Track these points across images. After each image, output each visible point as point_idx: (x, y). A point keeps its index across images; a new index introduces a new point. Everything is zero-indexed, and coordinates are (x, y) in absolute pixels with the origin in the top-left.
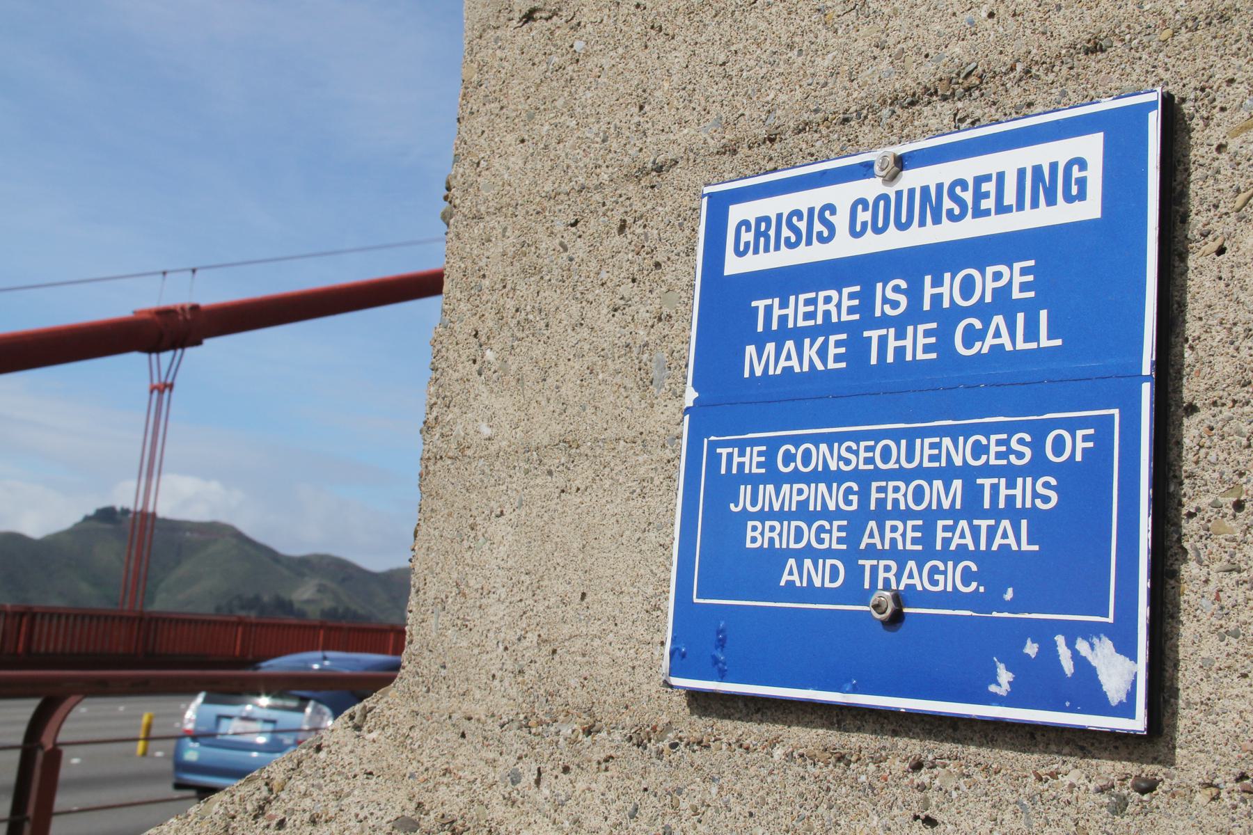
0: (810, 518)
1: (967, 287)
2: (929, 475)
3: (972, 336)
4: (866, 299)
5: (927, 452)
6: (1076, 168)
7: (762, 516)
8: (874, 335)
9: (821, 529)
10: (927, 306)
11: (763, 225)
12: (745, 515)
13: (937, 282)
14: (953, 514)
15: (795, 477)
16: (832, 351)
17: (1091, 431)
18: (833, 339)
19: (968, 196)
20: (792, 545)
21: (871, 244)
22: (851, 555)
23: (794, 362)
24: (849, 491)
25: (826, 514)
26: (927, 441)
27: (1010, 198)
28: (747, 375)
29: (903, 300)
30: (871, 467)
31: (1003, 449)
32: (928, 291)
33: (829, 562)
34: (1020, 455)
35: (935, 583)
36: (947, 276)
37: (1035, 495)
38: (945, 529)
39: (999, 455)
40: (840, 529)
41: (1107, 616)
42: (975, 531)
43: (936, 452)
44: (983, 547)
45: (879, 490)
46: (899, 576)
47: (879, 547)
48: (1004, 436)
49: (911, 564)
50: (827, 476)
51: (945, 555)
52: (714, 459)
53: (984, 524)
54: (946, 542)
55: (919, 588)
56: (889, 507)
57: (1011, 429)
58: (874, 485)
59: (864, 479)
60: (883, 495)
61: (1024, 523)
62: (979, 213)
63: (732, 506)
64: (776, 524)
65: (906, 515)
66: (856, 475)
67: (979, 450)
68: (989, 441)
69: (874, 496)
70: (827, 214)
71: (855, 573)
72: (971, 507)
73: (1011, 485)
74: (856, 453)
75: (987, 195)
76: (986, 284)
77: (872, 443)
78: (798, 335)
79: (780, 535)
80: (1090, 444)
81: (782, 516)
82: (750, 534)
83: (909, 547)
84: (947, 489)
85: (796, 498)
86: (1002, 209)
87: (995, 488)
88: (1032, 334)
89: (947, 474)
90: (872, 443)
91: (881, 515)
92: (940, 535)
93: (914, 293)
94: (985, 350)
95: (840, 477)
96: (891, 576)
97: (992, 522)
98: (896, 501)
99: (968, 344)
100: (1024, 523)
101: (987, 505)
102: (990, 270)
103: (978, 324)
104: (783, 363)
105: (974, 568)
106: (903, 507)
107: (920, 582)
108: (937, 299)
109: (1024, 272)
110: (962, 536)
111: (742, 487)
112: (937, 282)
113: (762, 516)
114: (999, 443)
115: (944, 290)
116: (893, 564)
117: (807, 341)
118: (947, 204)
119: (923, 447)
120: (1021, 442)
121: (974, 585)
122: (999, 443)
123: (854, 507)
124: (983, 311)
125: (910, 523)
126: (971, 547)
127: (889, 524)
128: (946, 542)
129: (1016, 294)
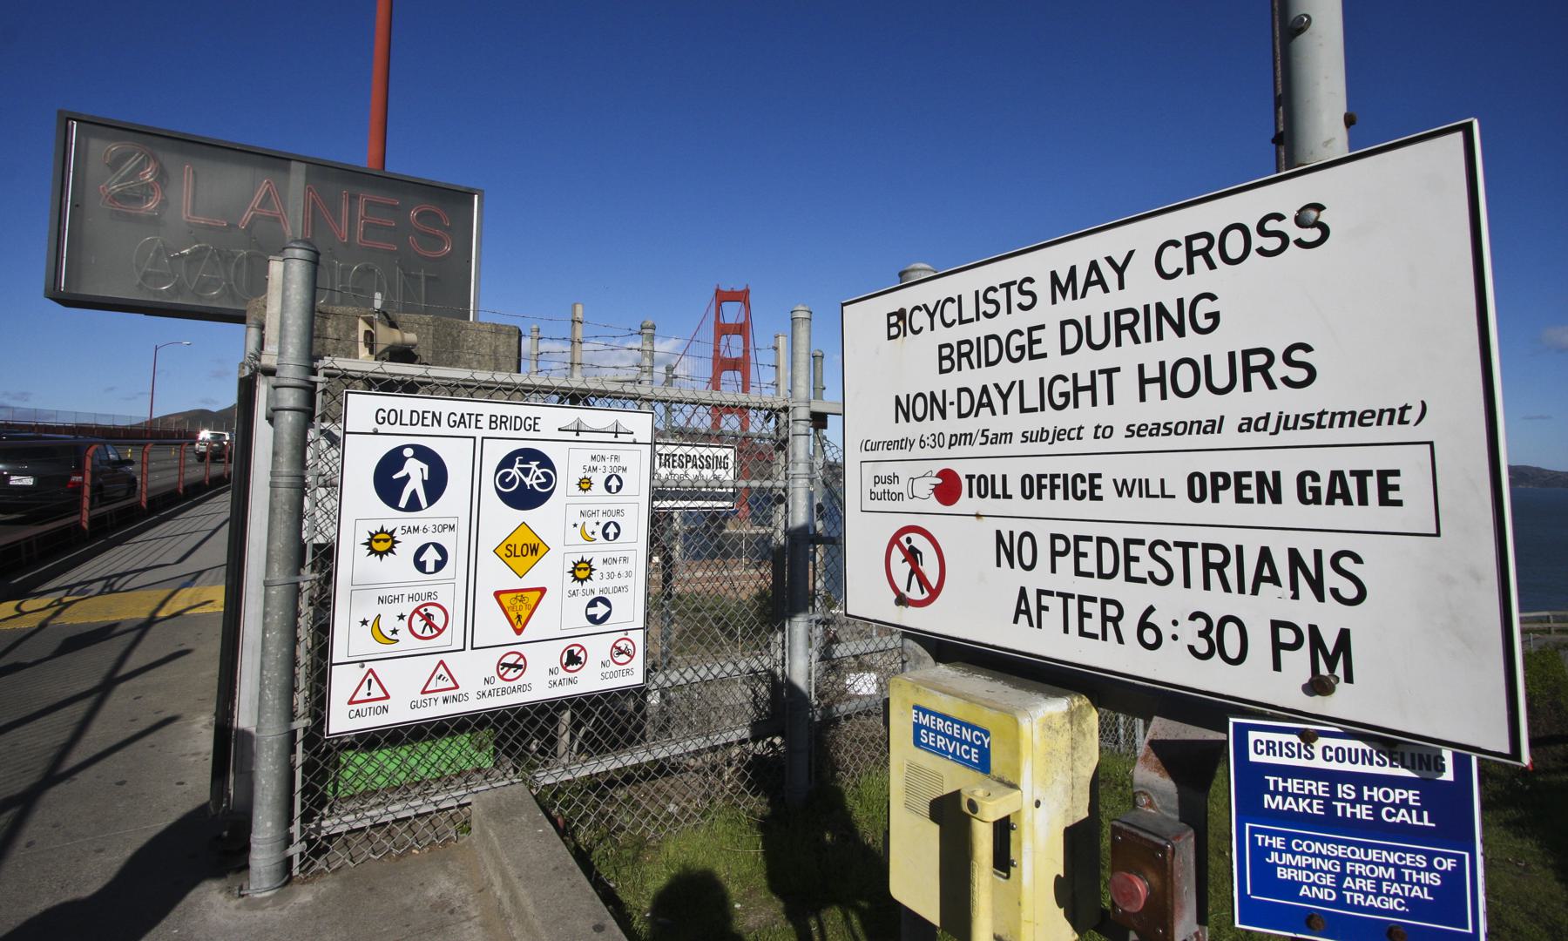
0: (1314, 872)
1: (1386, 795)
2: (1378, 864)
3: (1389, 814)
5: (1375, 856)
7: (1285, 866)
8: (1339, 805)
10: (1366, 798)
11: (1271, 745)
12: (1275, 865)
13: (1370, 790)
14: (1390, 880)
15: (1303, 853)
16: (1315, 807)
17: (1455, 861)
18: (1315, 802)
20: (1305, 880)
21: (1334, 766)
22: (1339, 889)
23: (1294, 806)
24: (1334, 864)
25: (1321, 870)
26: (1375, 851)
28: (1266, 806)
29: (1353, 795)
32: (1366, 793)
33: (1326, 890)
34: (1421, 864)
35: (1384, 905)
36: (1375, 789)
38: (1387, 885)
39: (1411, 862)
41: (1235, 724)
42: (1403, 889)
44: (1407, 894)
45: (1351, 866)
46: (1365, 900)
47: (1353, 888)
49: (1371, 897)
50: (1320, 855)
51: (1388, 894)
52: (1253, 841)
53: (1407, 887)
54: (1388, 891)
56: (1357, 873)
57: (1417, 852)
58: (1348, 864)
59: (1343, 862)
60: (1353, 868)
61: (1425, 889)
63: (1267, 860)
65: (1367, 878)
66: (1337, 858)
67: (1401, 858)
71: (1341, 898)
72: (1400, 878)
73: (1418, 873)
74: (1337, 849)
76: (1396, 795)
78: (1296, 797)
79: (1298, 875)
80: (1455, 865)
81: (1297, 867)
82: (1279, 873)
83: (1369, 890)
85: (1304, 862)
88: (1420, 818)
89: (1387, 865)
92: (1385, 889)
93: (1359, 793)
94: (1398, 821)
95: (1329, 858)
96: (1361, 900)
97: (1410, 886)
98: (1360, 872)
101: (1407, 879)
102: (1397, 791)
103: (1393, 811)
105: (1403, 902)
106: (1364, 874)
107: (1377, 904)
108: (1371, 797)
111: (1272, 853)
112: (1370, 790)
113: (1285, 866)
116: (1362, 896)
117: (1300, 800)
119: (1373, 854)
121: (1403, 908)
122: (1411, 857)
123: (1338, 870)
124: (1397, 807)
125: (1369, 881)
126: (1401, 894)
127: (1357, 880)
128: (1388, 891)
129: (1411, 803)
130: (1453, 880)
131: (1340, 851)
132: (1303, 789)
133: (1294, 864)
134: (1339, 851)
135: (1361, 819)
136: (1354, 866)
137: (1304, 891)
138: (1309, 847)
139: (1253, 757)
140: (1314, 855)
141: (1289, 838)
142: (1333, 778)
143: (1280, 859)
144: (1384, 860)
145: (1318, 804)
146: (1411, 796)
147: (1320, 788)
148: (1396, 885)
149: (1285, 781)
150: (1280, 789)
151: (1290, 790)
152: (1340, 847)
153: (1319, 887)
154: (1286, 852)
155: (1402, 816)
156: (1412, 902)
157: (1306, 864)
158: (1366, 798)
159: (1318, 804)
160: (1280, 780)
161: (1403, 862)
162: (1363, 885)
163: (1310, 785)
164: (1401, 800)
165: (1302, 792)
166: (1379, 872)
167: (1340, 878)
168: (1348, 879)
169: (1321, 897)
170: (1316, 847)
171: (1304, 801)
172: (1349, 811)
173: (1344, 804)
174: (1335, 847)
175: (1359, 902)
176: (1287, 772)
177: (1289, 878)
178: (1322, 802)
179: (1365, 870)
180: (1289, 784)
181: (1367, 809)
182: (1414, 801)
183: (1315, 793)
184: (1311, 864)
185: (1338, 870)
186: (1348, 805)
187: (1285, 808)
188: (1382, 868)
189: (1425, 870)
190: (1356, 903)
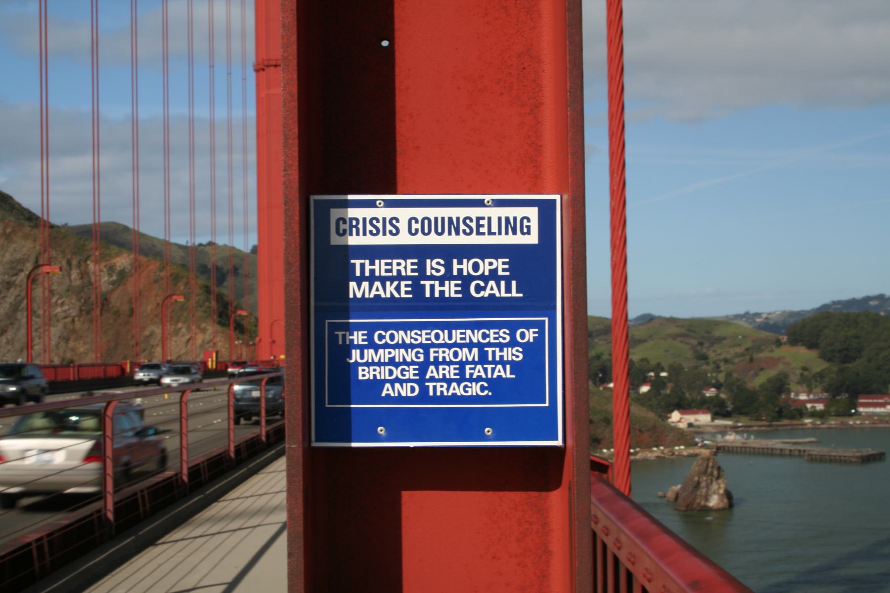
0: (397, 365)
1: (476, 267)
2: (461, 346)
3: (478, 289)
4: (421, 268)
5: (459, 336)
6: (525, 221)
7: (367, 364)
8: (427, 284)
9: (403, 370)
10: (455, 273)
11: (354, 223)
12: (357, 364)
13: (460, 263)
14: (473, 362)
15: (386, 346)
16: (403, 289)
19: (473, 225)
20: (387, 377)
21: (420, 240)
22: (421, 381)
23: (381, 292)
24: (418, 353)
25: (405, 362)
26: (459, 331)
27: (495, 228)
28: (351, 296)
29: (443, 270)
30: (430, 342)
31: (497, 336)
33: (409, 385)
34: (504, 339)
35: (467, 392)
36: (465, 261)
37: (513, 355)
38: (471, 369)
39: (495, 338)
40: (414, 369)
42: (485, 370)
43: (463, 336)
44: (489, 376)
45: (435, 352)
46: (448, 389)
47: (437, 377)
48: (497, 331)
49: (454, 384)
51: (471, 380)
53: (489, 367)
54: (471, 374)
55: (459, 394)
56: (441, 359)
58: (432, 350)
59: (426, 348)
60: (437, 355)
61: (508, 367)
62: (478, 233)
64: (377, 368)
65: (450, 363)
66: (421, 345)
68: (489, 331)
69: (432, 355)
70: (394, 222)
71: (424, 390)
72: (483, 359)
73: (502, 351)
75: (483, 226)
76: (485, 267)
77: (429, 331)
78: (383, 280)
79: (380, 373)
80: (536, 335)
81: (380, 364)
82: (360, 373)
83: (452, 377)
84: (470, 352)
85: (387, 356)
86: (490, 233)
87: (494, 353)
88: (508, 290)
89: (470, 346)
90: (429, 331)
91: (437, 363)
92: (468, 372)
93: (448, 267)
94: (486, 295)
95: (412, 346)
96: (444, 389)
97: (494, 366)
98: (444, 358)
99: (478, 291)
100: (508, 367)
101: (490, 359)
102: (487, 261)
103: (482, 284)
104: (374, 292)
105: (486, 385)
106: (448, 360)
107: (460, 392)
108: (460, 271)
109: (504, 263)
110: (479, 372)
111: (354, 351)
112: (460, 263)
113: (367, 364)
114: (495, 333)
115: (464, 267)
116: (445, 385)
117: (388, 283)
118: (462, 227)
119: (457, 335)
120: (504, 333)
121: (486, 392)
122: (495, 333)
123: (422, 359)
125: (452, 367)
126: (484, 376)
127: (441, 367)
128: (471, 374)
129: (500, 273)
130: (533, 351)
131: (424, 336)
132: (390, 271)
133: (376, 360)
134: (423, 337)
135: (450, 298)
136: (437, 352)
137: (387, 390)
138: (392, 337)
139: (335, 240)
140: (397, 346)
141: (371, 329)
142: (421, 253)
143: (362, 357)
144: (468, 341)
145: (406, 286)
146: (500, 265)
147: (407, 267)
148: (479, 367)
149: (372, 263)
150: (367, 274)
151: (377, 274)
152: (424, 332)
153: (401, 382)
154: (368, 347)
155: (492, 289)
156: (495, 384)
157: (390, 358)
158: (455, 273)
159: (406, 286)
160: (367, 262)
161: (487, 340)
162: (446, 372)
163: (399, 264)
164: (490, 270)
165: (390, 274)
166: (463, 354)
167: (423, 368)
168: (432, 368)
169: (403, 394)
170: (400, 336)
171: (391, 284)
172: (437, 289)
173: (432, 282)
174: (419, 332)
175: (442, 392)
176: (373, 253)
177: (372, 378)
178: (410, 282)
179: (449, 354)
180: (376, 267)
181: (456, 285)
182: (504, 270)
183: (403, 274)
184: (394, 358)
185: (422, 359)
186: (437, 283)
187: (372, 296)
188: (465, 350)
189: (507, 345)
190: (438, 394)
